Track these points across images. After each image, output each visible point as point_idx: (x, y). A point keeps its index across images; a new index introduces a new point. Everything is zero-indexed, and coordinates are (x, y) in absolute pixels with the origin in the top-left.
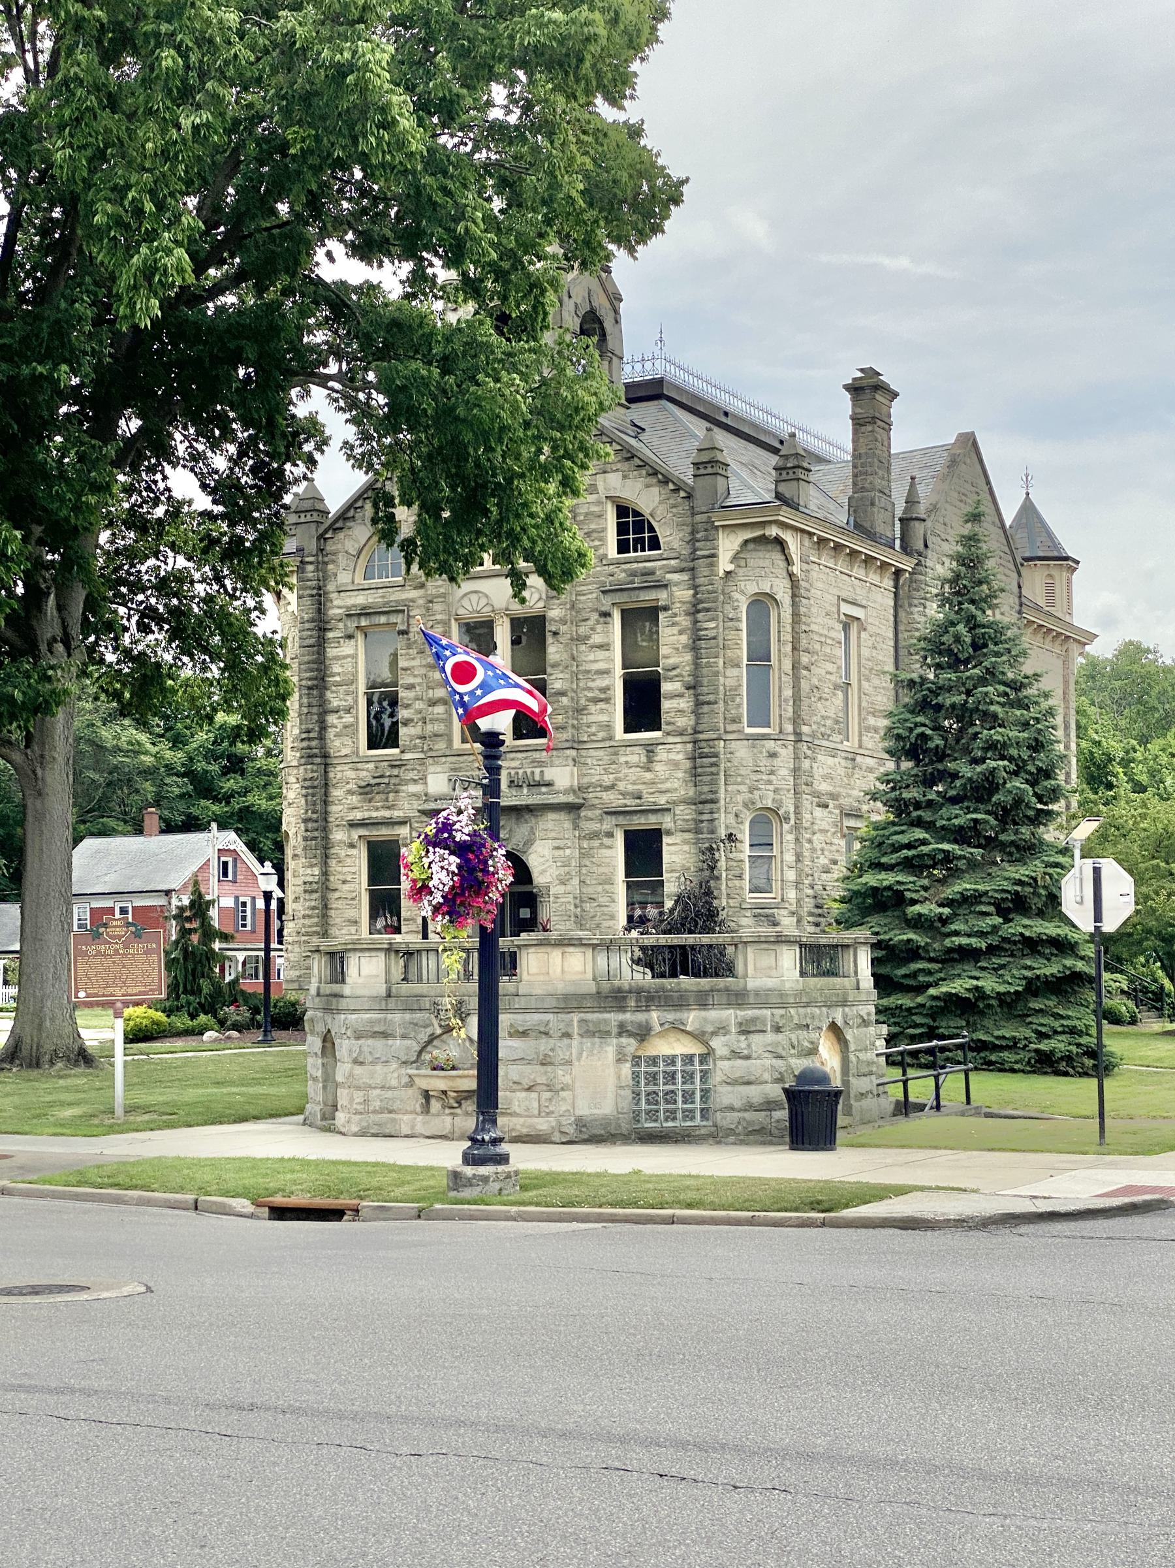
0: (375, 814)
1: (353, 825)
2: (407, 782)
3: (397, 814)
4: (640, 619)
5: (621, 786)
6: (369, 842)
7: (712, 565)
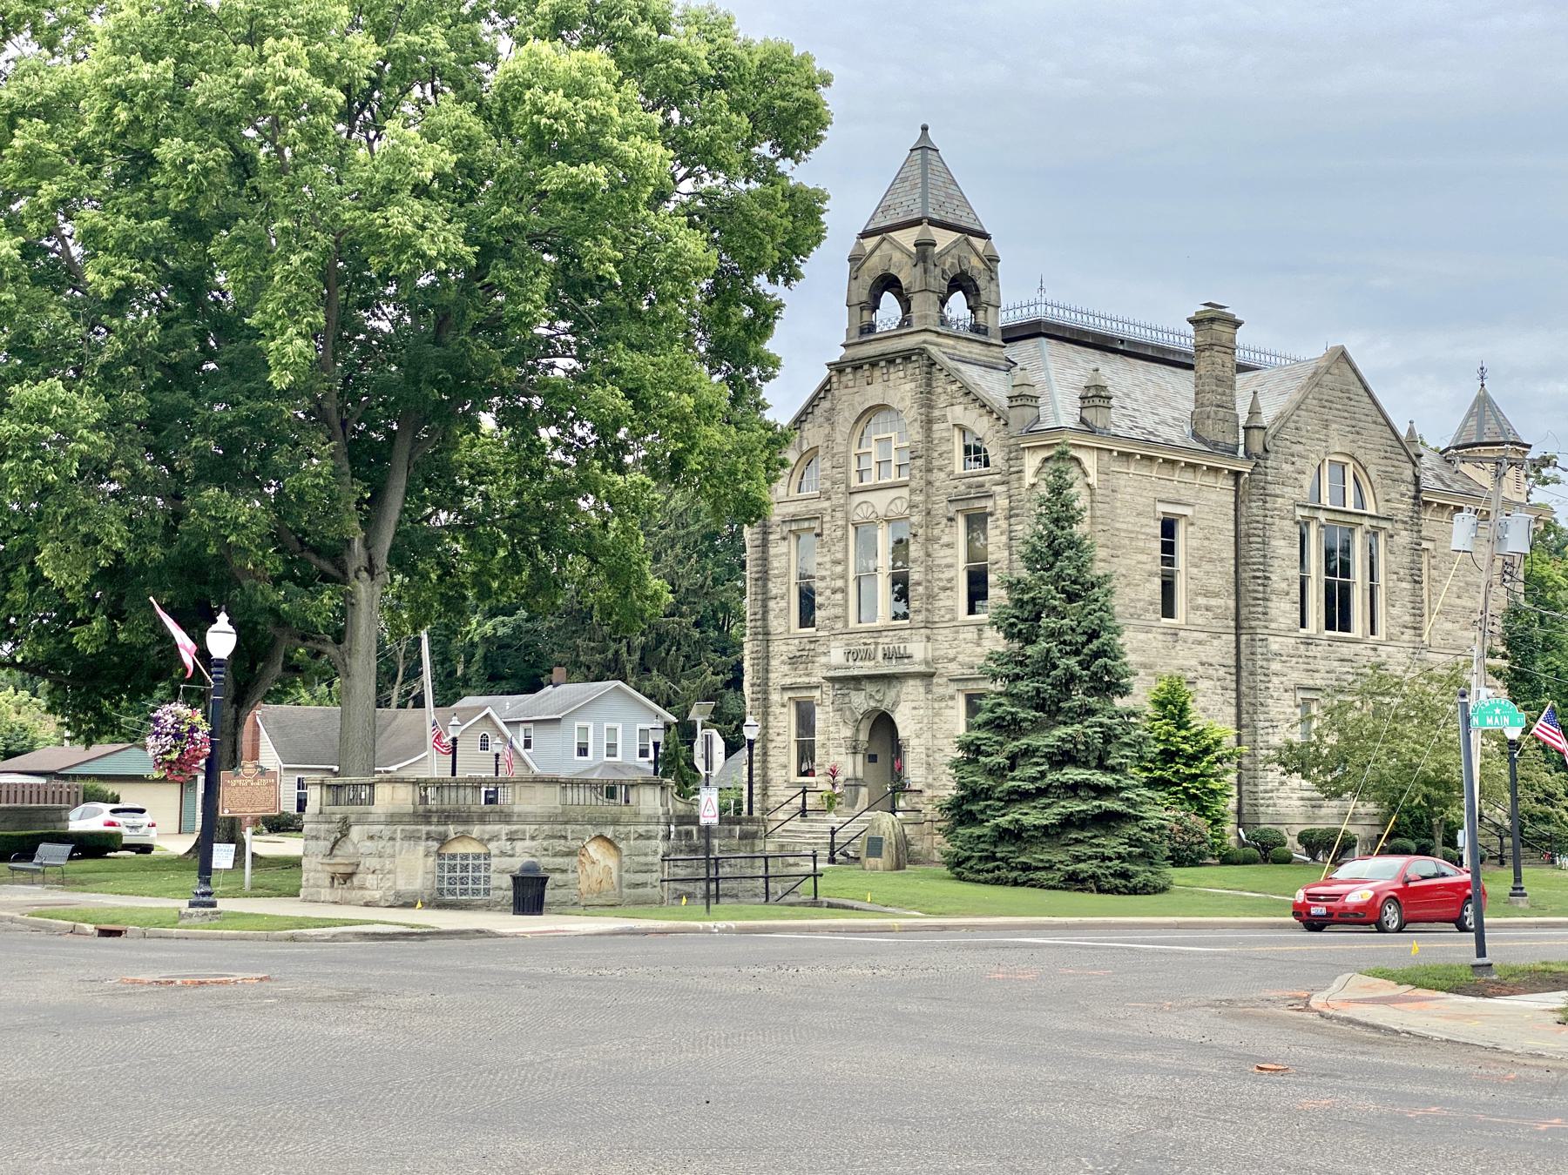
1: (784, 689)
3: (814, 680)
4: (977, 521)
5: (961, 658)
6: (798, 704)
7: (1020, 479)
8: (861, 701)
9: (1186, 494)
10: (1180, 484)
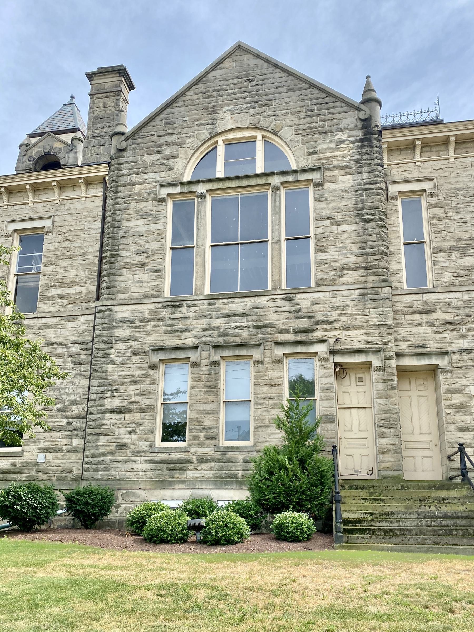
9: (41, 210)
10: (29, 205)
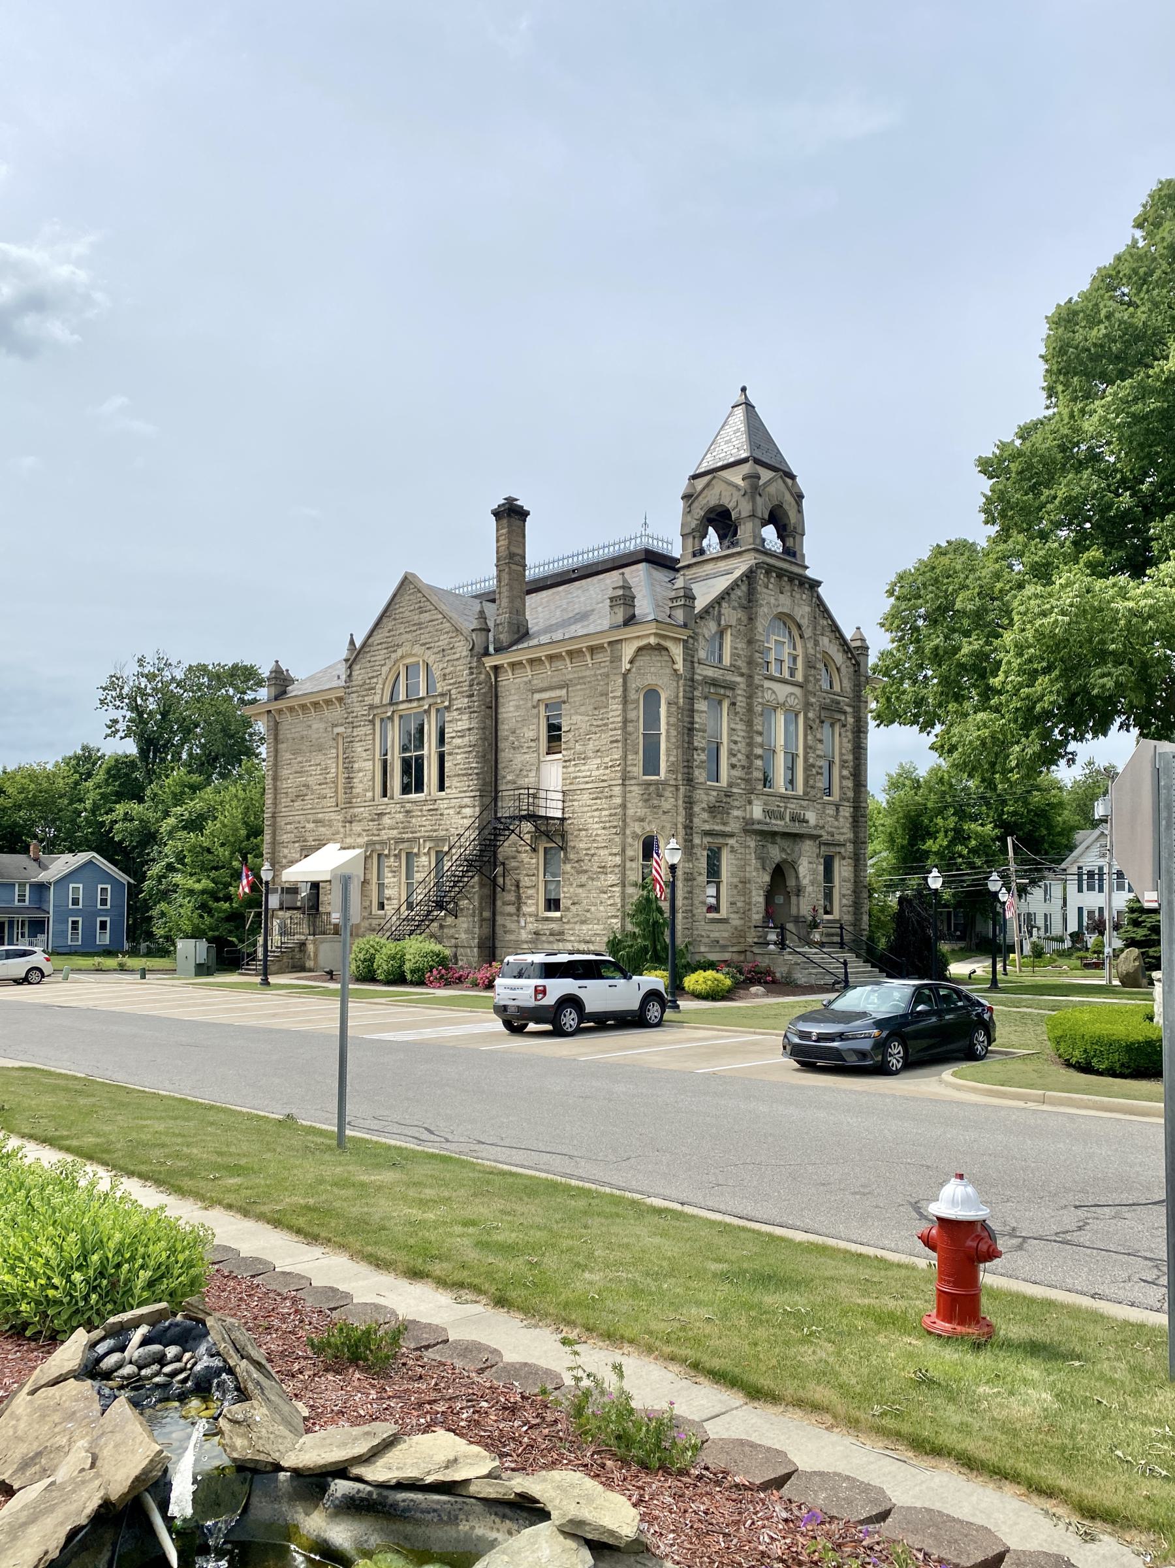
0: (717, 828)
1: (707, 833)
2: (733, 807)
3: (727, 829)
8: (775, 854)
